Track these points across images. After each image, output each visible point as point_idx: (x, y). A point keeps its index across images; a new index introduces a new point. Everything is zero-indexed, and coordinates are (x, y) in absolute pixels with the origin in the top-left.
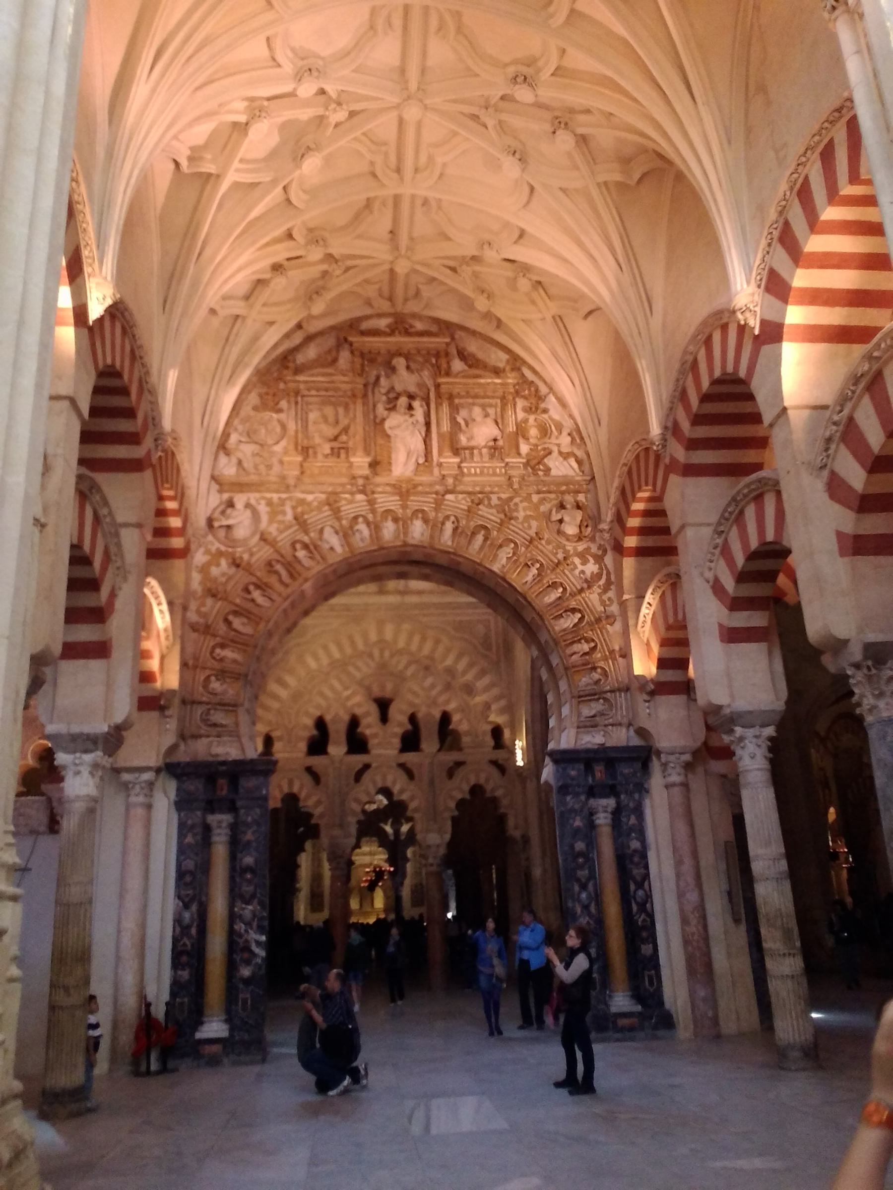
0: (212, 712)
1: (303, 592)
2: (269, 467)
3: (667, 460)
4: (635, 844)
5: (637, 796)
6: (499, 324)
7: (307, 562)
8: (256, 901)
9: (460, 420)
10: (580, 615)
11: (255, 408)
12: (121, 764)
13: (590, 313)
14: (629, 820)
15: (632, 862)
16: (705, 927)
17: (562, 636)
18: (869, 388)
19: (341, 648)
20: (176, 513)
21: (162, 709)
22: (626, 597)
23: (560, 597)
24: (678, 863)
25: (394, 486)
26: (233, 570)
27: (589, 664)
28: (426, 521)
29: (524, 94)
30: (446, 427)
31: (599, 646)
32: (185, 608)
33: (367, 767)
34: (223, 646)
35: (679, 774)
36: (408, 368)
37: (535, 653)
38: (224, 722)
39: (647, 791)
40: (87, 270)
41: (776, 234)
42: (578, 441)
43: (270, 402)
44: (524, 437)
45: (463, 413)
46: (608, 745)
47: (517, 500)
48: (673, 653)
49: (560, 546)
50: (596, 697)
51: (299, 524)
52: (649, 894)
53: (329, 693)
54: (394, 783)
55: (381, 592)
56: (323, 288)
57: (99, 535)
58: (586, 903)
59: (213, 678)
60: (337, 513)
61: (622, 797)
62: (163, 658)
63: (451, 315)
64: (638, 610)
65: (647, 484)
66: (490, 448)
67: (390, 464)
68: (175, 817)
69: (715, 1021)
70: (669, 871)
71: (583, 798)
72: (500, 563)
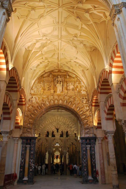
2: (38, 92)
3: (98, 91)
4: (93, 153)
5: (94, 145)
6: (74, 71)
7: (43, 106)
9: (68, 85)
10: (85, 116)
11: (37, 83)
12: (14, 136)
13: (88, 69)
15: (93, 156)
16: (104, 166)
18: (124, 80)
19: (51, 120)
20: (24, 98)
21: (20, 128)
22: (93, 113)
23: (82, 113)
24: (100, 156)
25: (57, 95)
28: (62, 100)
29: (75, 39)
30: (66, 86)
32: (25, 113)
34: (30, 119)
35: (100, 141)
36: (60, 77)
39: (95, 144)
40: (9, 63)
41: (111, 58)
42: (86, 88)
43: (39, 82)
45: (68, 84)
47: (76, 97)
48: (99, 122)
49: (83, 105)
53: (49, 128)
54: (59, 142)
55: (58, 112)
56: (48, 66)
57: (10, 101)
58: (85, 162)
59: (28, 124)
60: (48, 99)
61: (92, 145)
62: (21, 120)
63: (67, 69)
64: (95, 115)
66: (72, 89)
67: (57, 91)
68: (21, 145)
69: (105, 181)
71: (85, 145)
72: (73, 107)
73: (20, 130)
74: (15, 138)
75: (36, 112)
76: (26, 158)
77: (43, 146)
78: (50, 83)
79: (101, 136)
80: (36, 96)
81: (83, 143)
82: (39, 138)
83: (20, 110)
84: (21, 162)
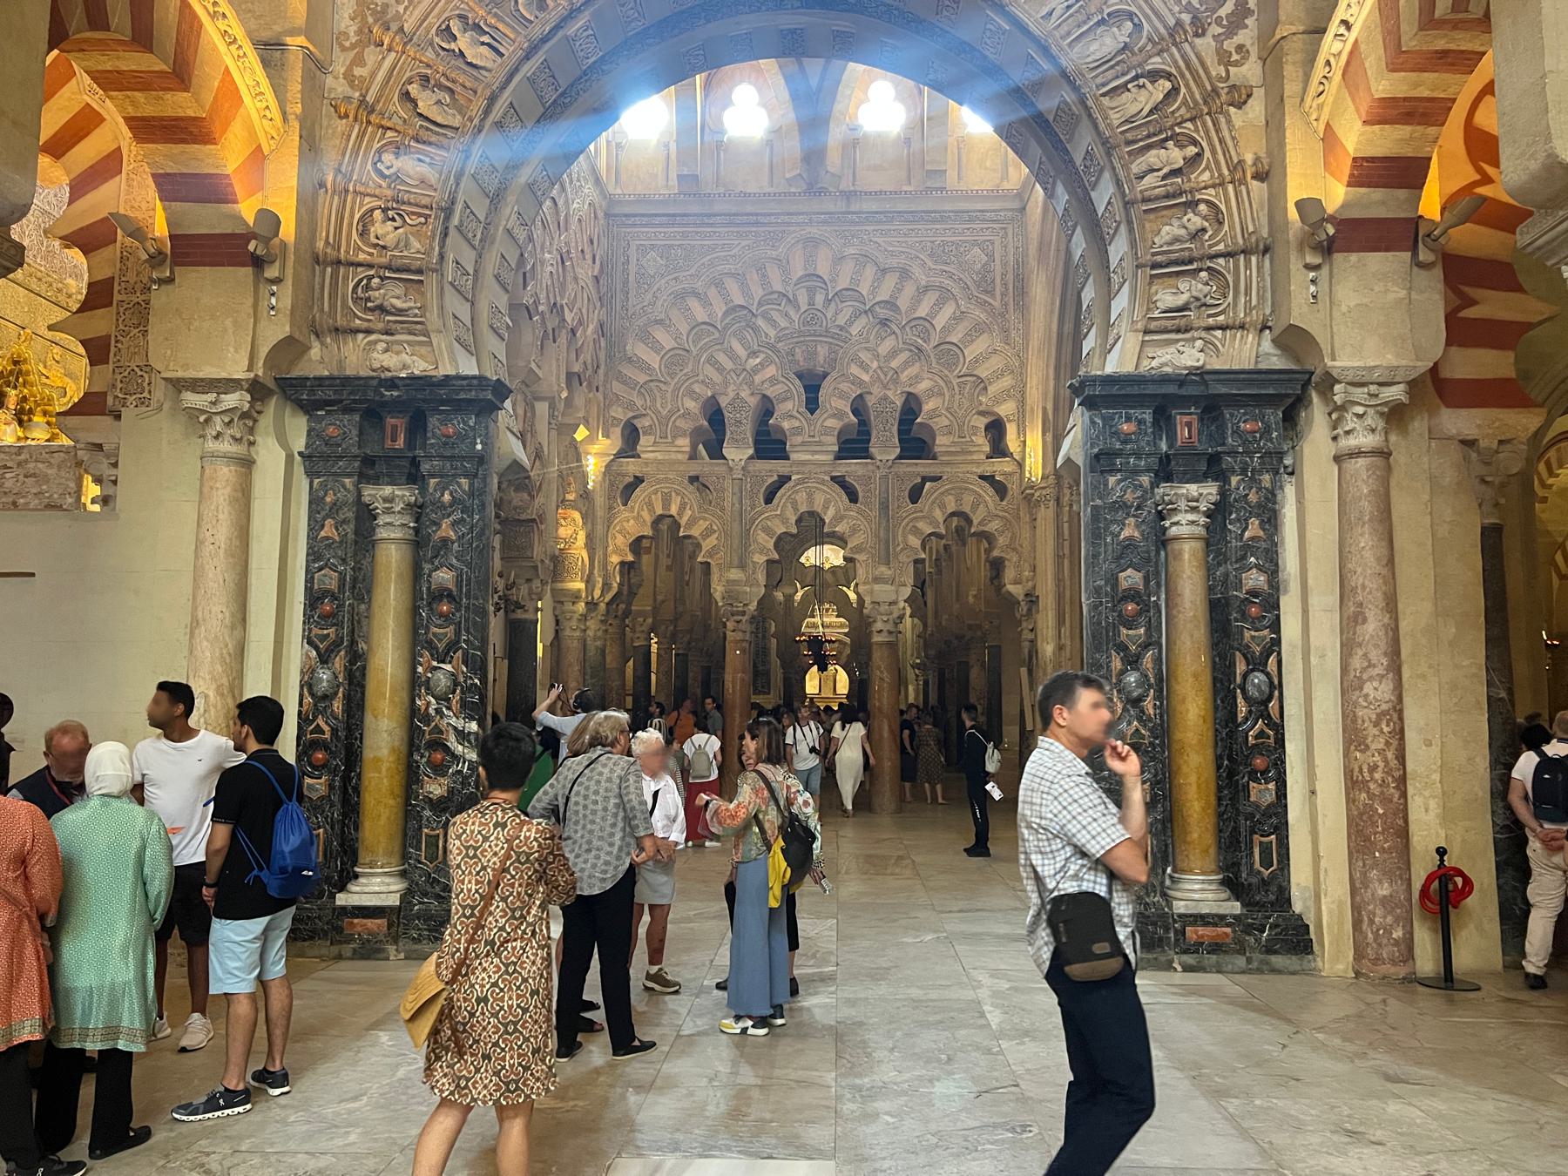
0: (376, 281)
4: (1255, 579)
5: (1266, 478)
8: (460, 653)
10: (1168, 85)
14: (1244, 531)
15: (1244, 616)
16: (1401, 757)
17: (1121, 133)
21: (258, 263)
23: (1126, 47)
24: (1350, 621)
27: (1181, 194)
31: (1207, 154)
32: (316, 66)
33: (784, 480)
34: (398, 149)
35: (1373, 431)
38: (398, 303)
46: (1208, 367)
50: (1194, 266)
52: (1276, 682)
53: (728, 365)
59: (378, 214)
61: (1234, 480)
64: (1310, 61)
68: (302, 485)
70: (1326, 636)
71: (1145, 480)
74: (198, 385)
76: (367, 639)
79: (1390, 359)
81: (1118, 453)
82: (631, 467)
84: (312, 694)
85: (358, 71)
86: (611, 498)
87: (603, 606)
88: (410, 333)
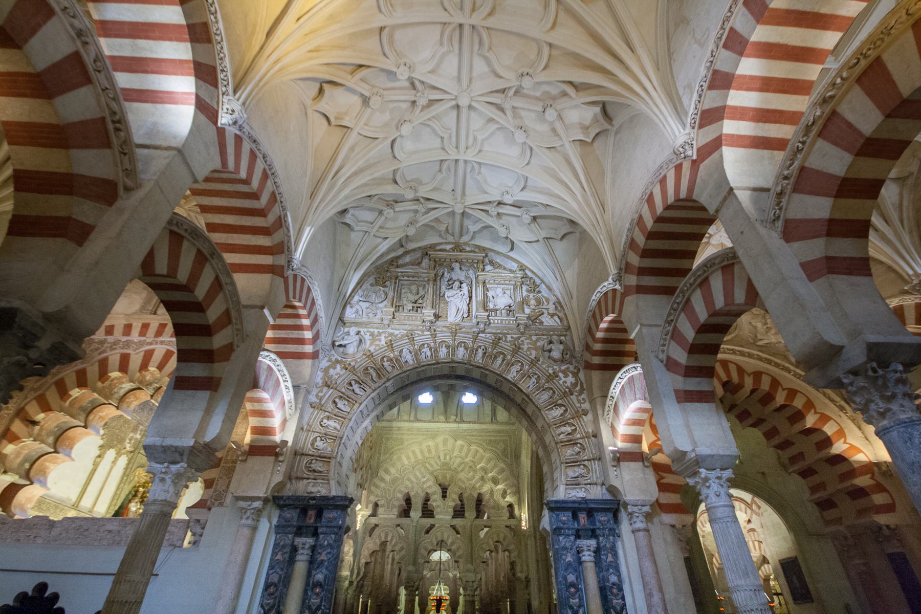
0: (314, 461)
1: (386, 387)
7: (389, 369)
9: (489, 294)
19: (422, 452)
21: (277, 455)
26: (344, 371)
28: (466, 348)
30: (480, 297)
32: (308, 392)
33: (432, 526)
34: (328, 418)
36: (461, 269)
37: (534, 437)
44: (527, 305)
47: (523, 338)
51: (388, 346)
54: (448, 539)
55: (447, 422)
59: (318, 439)
64: (604, 405)
65: (607, 315)
73: (277, 461)
75: (357, 390)
77: (390, 560)
78: (421, 289)
80: (360, 329)
82: (374, 520)
83: (286, 372)
85: (321, 394)
86: (364, 533)
87: (355, 583)
88: (323, 479)
